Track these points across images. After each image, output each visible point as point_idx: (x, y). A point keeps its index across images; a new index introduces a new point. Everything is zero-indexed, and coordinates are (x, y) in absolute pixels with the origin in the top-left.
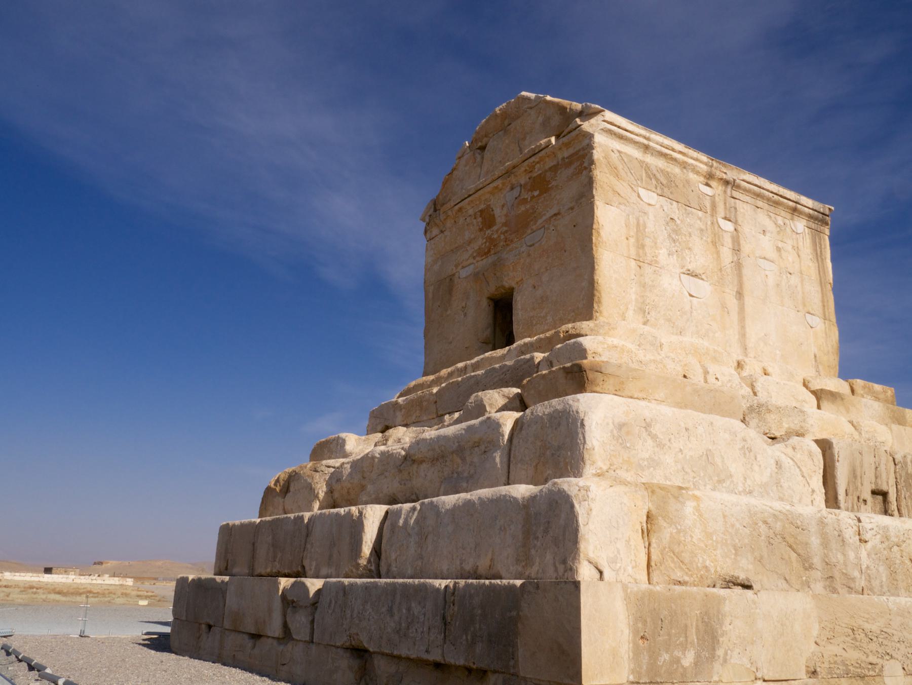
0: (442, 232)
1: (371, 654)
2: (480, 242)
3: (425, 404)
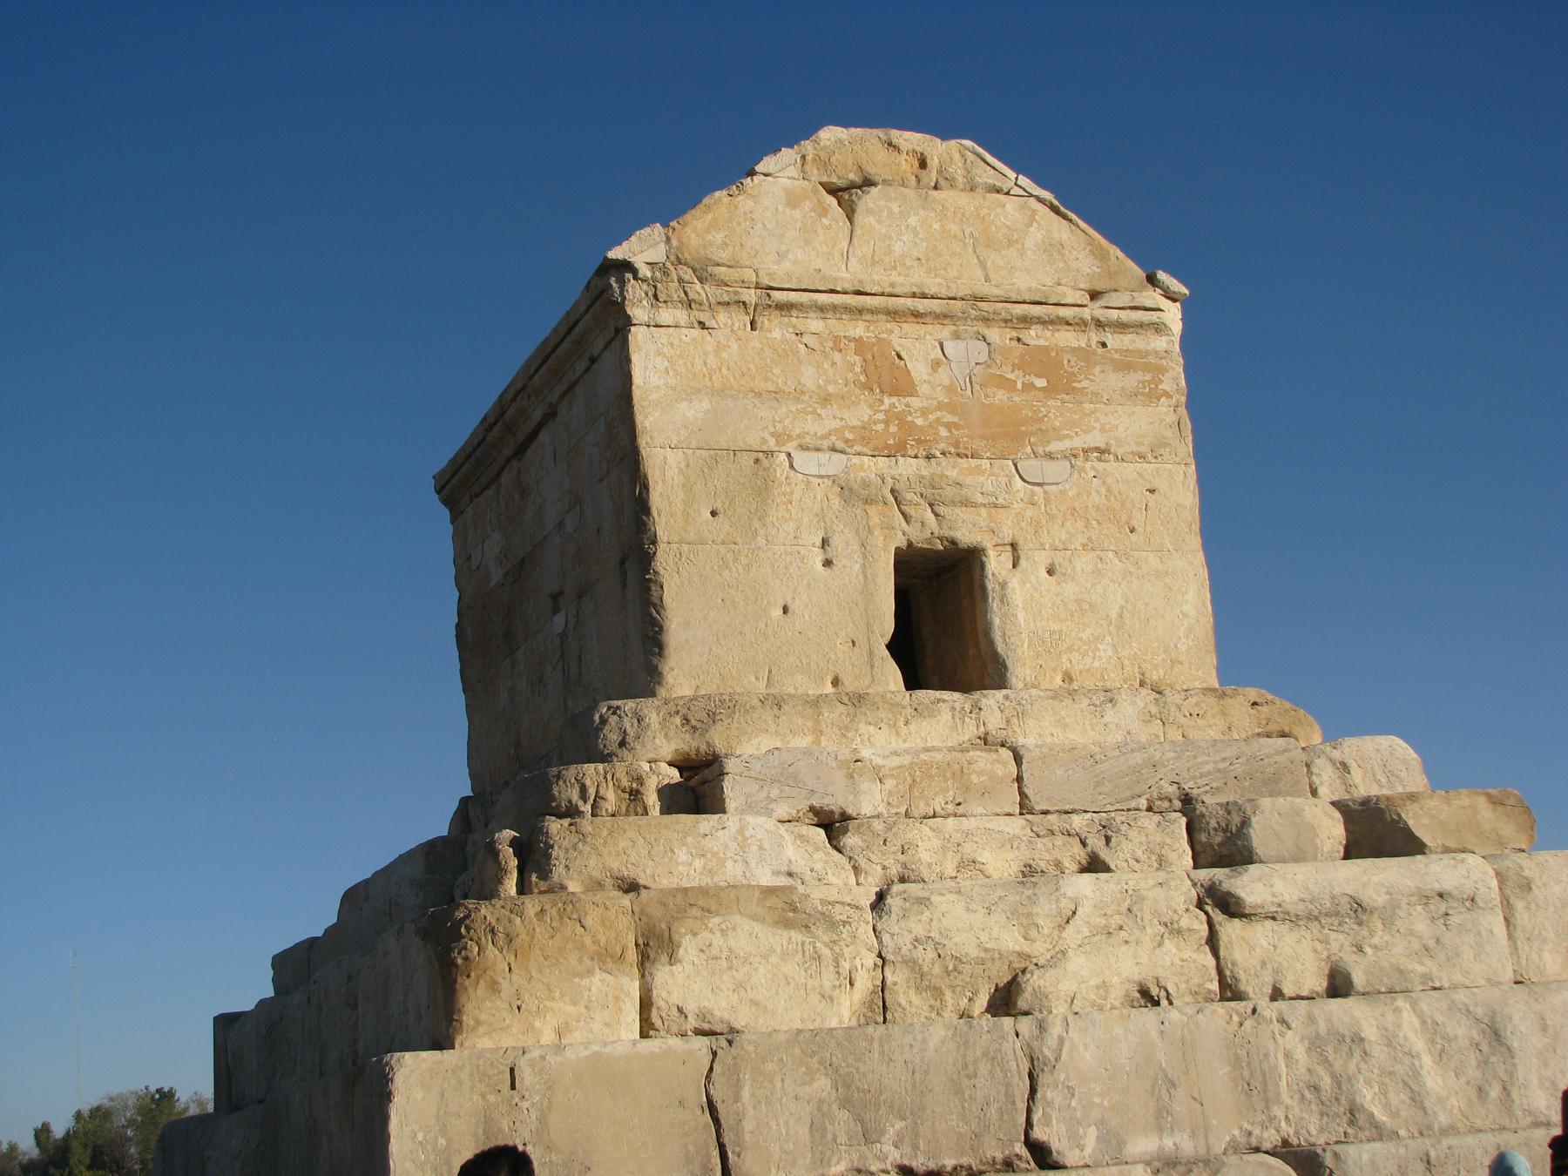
0: (702, 325)
2: (861, 413)
3: (974, 778)
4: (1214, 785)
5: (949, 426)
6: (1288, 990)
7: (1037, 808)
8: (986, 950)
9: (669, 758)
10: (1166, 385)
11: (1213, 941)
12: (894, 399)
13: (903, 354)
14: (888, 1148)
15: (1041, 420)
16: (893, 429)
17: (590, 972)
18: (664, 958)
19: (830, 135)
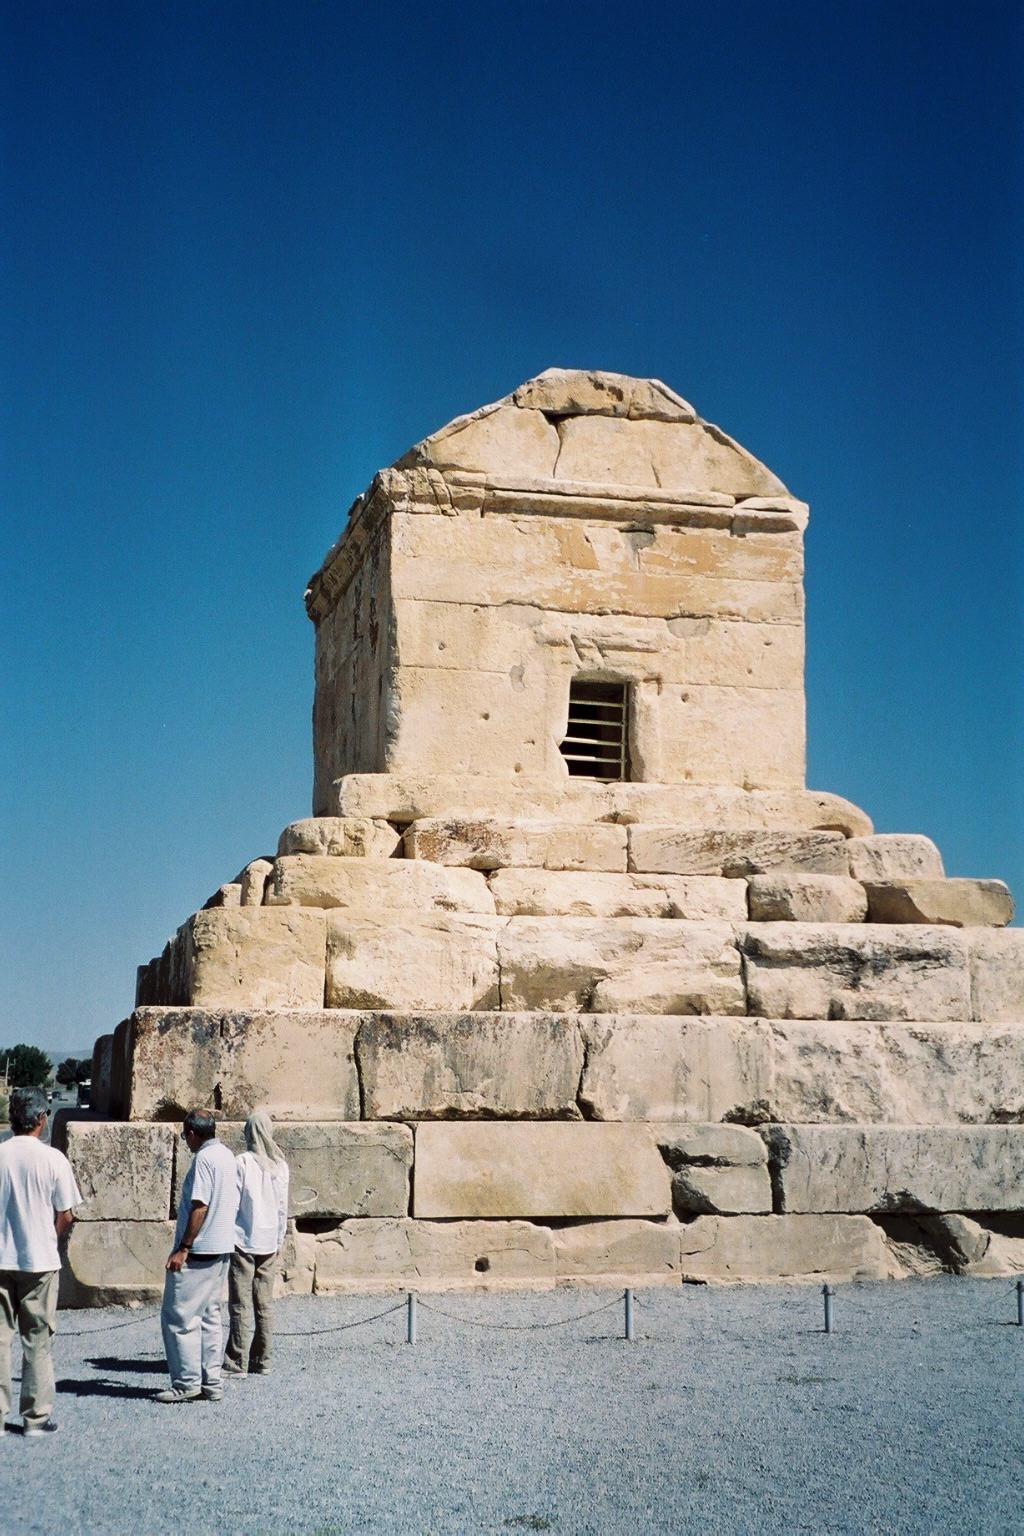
0: (444, 512)
1: (933, 1213)
4: (774, 862)
5: (618, 591)
6: (797, 1011)
7: (639, 869)
8: (574, 965)
9: (387, 817)
10: (789, 567)
11: (743, 972)
12: (581, 571)
13: (589, 538)
14: (477, 1096)
15: (690, 589)
16: (578, 592)
17: (291, 961)
18: (344, 955)
19: (551, 374)
